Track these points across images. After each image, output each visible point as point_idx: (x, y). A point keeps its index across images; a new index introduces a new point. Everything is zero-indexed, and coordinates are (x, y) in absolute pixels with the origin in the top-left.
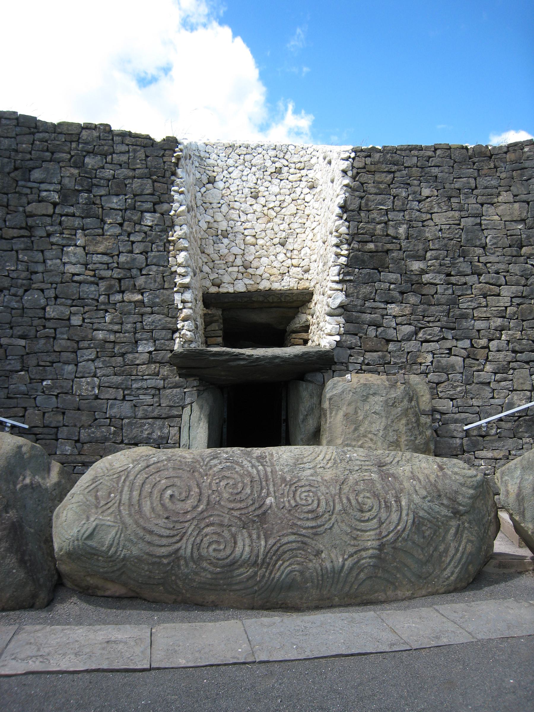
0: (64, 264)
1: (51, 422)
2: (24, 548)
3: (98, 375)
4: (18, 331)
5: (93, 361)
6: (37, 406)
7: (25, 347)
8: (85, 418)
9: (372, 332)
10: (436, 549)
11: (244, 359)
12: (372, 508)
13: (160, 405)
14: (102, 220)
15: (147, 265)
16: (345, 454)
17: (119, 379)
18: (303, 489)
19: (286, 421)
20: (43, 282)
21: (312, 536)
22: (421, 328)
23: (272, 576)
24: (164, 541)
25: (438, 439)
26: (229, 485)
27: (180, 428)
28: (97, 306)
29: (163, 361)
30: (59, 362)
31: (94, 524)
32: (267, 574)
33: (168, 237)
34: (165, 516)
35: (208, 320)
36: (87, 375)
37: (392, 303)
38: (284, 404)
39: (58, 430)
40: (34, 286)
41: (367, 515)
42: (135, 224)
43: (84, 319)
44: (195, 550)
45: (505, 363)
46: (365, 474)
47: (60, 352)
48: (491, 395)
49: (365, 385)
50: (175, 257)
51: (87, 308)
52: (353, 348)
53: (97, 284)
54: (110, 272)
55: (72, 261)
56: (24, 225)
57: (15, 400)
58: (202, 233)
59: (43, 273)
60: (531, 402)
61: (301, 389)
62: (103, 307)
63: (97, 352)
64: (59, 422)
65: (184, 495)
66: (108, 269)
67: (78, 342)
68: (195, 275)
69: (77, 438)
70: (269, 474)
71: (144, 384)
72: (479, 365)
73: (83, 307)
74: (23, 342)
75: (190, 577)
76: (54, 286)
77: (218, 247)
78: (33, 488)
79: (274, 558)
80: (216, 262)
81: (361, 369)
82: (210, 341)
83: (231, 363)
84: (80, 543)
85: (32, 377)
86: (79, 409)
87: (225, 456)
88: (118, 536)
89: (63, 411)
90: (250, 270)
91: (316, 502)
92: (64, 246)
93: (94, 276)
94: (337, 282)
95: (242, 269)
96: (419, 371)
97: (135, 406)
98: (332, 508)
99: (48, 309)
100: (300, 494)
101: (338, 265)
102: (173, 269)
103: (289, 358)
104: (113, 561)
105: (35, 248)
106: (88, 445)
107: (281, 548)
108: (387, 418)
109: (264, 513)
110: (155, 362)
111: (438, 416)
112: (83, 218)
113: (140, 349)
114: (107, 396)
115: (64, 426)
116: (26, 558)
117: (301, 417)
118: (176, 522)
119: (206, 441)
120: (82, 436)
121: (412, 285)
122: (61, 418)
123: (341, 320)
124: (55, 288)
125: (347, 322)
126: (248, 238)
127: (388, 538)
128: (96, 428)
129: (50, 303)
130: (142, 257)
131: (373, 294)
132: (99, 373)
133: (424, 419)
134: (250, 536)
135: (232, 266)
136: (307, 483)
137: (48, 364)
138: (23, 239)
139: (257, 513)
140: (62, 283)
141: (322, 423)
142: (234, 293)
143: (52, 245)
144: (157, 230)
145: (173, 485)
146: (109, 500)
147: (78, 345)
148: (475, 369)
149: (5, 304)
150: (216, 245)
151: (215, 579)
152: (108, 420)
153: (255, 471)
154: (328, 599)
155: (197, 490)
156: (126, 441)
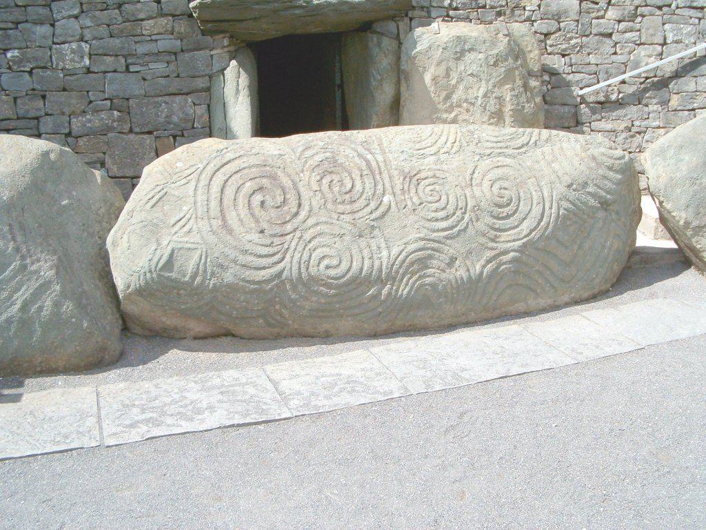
1: (28, 111)
3: (86, 38)
5: (76, 17)
6: (3, 90)
10: (580, 247)
12: (511, 201)
13: (178, 76)
16: (472, 133)
17: (117, 42)
19: (341, 86)
21: (444, 240)
24: (264, 262)
25: (546, 107)
26: (334, 182)
27: (209, 106)
29: (178, 13)
30: (27, 21)
31: (169, 248)
36: (70, 39)
38: (337, 65)
39: (38, 122)
41: (506, 210)
44: (303, 270)
45: (632, 8)
46: (500, 158)
47: (25, 6)
48: (613, 50)
49: (458, 37)
60: (661, 59)
61: (370, 44)
64: (39, 110)
69: (67, 131)
70: (382, 165)
71: (152, 47)
72: (598, 11)
75: (299, 304)
81: (448, 16)
83: (282, 13)
84: (155, 275)
86: (64, 90)
88: (203, 261)
89: (43, 93)
91: (444, 197)
96: (523, 18)
97: (144, 79)
98: (464, 203)
108: (488, 81)
110: (166, 15)
111: (546, 78)
114: (103, 68)
115: (47, 114)
117: (374, 83)
118: (275, 236)
119: (250, 120)
120: (74, 127)
122: (42, 102)
127: (530, 237)
128: (93, 115)
132: (88, 36)
133: (534, 83)
136: (430, 174)
137: (11, 25)
139: (374, 216)
141: (403, 89)
146: (182, 215)
148: (594, 15)
151: (329, 303)
152: (108, 103)
153: (364, 164)
154: (463, 315)
155: (293, 192)
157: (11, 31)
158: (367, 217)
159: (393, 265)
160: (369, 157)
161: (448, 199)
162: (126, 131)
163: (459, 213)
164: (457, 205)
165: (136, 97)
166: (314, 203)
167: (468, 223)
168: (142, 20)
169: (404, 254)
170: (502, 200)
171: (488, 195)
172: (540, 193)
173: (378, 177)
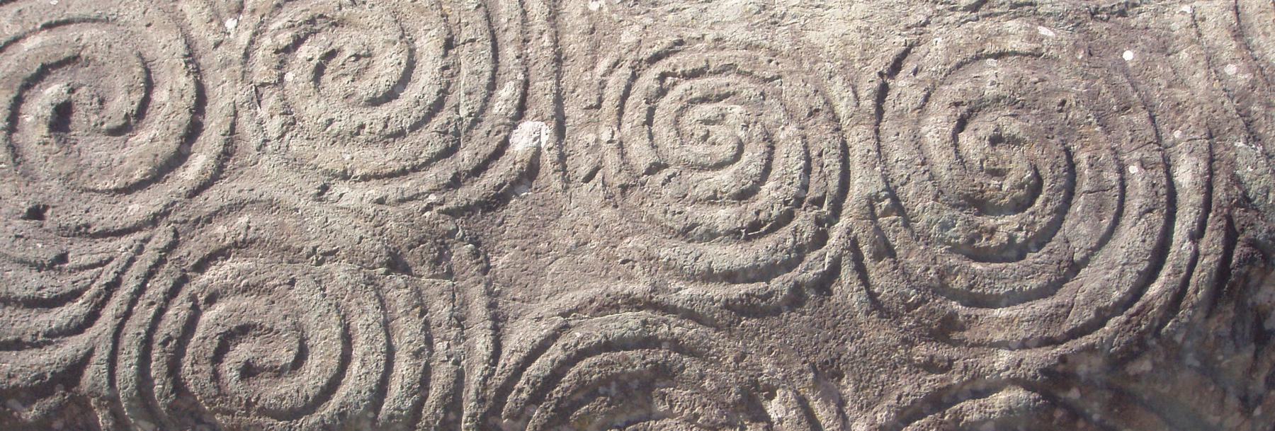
18: (699, 86)
26: (338, 60)
34: (25, 206)
44: (157, 368)
46: (1012, 25)
65: (121, 104)
98: (834, 184)
100: (683, 110)
109: (498, 199)
118: (82, 232)
134: (421, 305)
145: (73, 60)
155: (184, 81)
158: (432, 198)
159: (504, 391)
161: (770, 159)
163: (804, 221)
164: (805, 187)
166: (246, 125)
169: (556, 352)
170: (994, 182)
171: (942, 161)
172: (1161, 172)
173: (509, 53)
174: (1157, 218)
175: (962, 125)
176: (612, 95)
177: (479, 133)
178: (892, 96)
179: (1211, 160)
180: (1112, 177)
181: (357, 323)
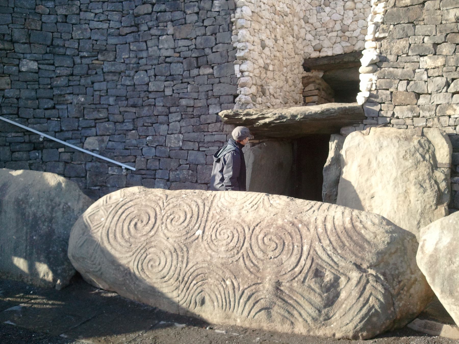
0: (160, 49)
2: (51, 249)
3: (182, 132)
4: (131, 102)
5: (179, 121)
6: (143, 155)
7: (135, 113)
8: (174, 164)
9: (402, 86)
11: (268, 117)
14: (185, 12)
15: (216, 44)
20: (147, 65)
22: (453, 80)
23: (188, 291)
28: (182, 80)
30: (157, 123)
32: (185, 289)
33: (231, 19)
35: (306, 81)
36: (175, 132)
37: (426, 55)
40: (141, 68)
42: (207, 11)
43: (173, 90)
47: (158, 116)
50: (237, 35)
51: (175, 82)
52: (384, 103)
53: (182, 63)
54: (190, 52)
55: (165, 46)
56: (133, 24)
57: (129, 151)
58: (307, 5)
59: (146, 58)
62: (185, 80)
63: (182, 115)
64: (157, 166)
66: (189, 50)
67: (169, 108)
68: (263, 47)
69: (167, 178)
73: (173, 81)
74: (134, 110)
76: (154, 67)
77: (321, 16)
78: (64, 211)
79: (190, 277)
80: (318, 30)
82: (308, 99)
85: (140, 134)
86: (169, 157)
87: (184, 196)
89: (159, 158)
90: (347, 34)
91: (230, 238)
92: (160, 36)
93: (180, 57)
94: (373, 41)
95: (340, 33)
97: (206, 155)
98: (241, 245)
99: (150, 84)
101: (373, 24)
102: (235, 45)
103: (311, 115)
104: (95, 264)
105: (141, 40)
106: (175, 183)
107: (196, 271)
112: (171, 12)
113: (211, 111)
115: (160, 169)
116: (51, 256)
120: (170, 176)
121: (447, 34)
122: (158, 163)
123: (374, 77)
124: (154, 69)
125: (378, 78)
126: (348, 3)
129: (151, 80)
130: (213, 38)
131: (407, 49)
135: (332, 31)
137: (150, 124)
138: (133, 34)
140: (158, 64)
142: (333, 56)
143: (152, 36)
144: (223, 14)
147: (169, 110)
149: (123, 83)
150: (319, 14)
156: (199, 181)
157: (150, 127)
160: (201, 207)
162: (195, 181)
165: (202, 164)
166: (160, 228)
167: (239, 258)
168: (209, 124)
169: (194, 268)
173: (199, 219)
174: (299, 256)
175: (265, 236)
176: (212, 227)
177: (192, 231)
178: (255, 230)
179: (311, 246)
180: (291, 247)
181: (168, 260)
